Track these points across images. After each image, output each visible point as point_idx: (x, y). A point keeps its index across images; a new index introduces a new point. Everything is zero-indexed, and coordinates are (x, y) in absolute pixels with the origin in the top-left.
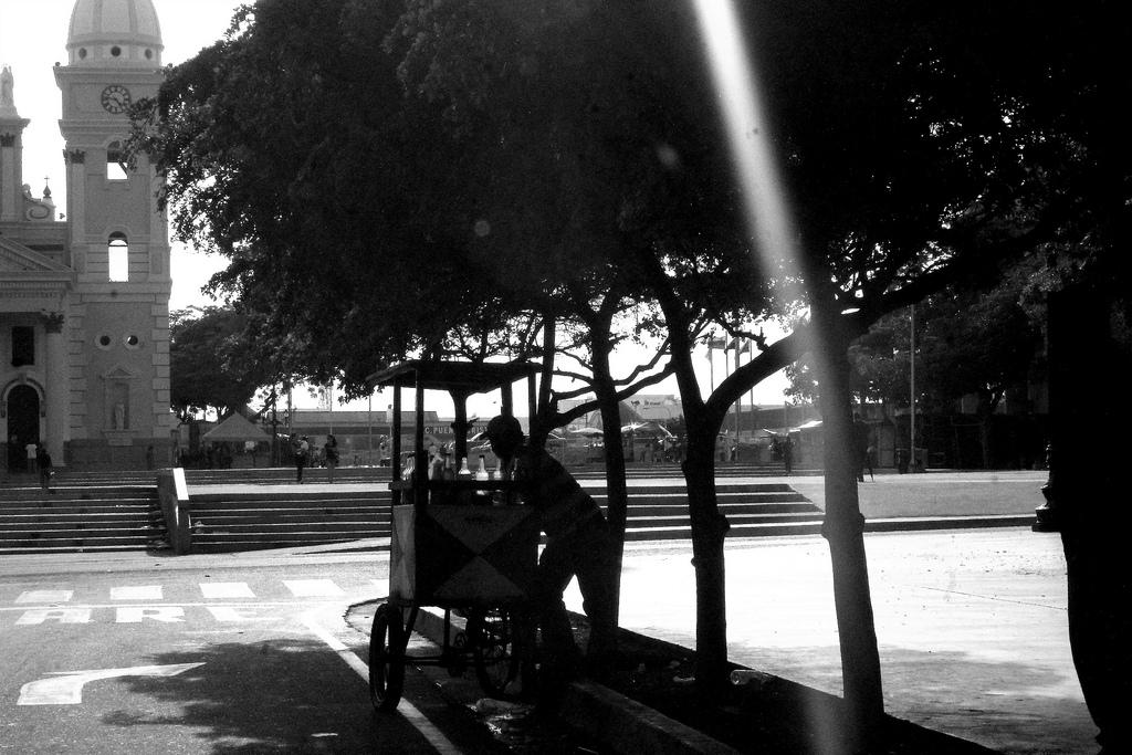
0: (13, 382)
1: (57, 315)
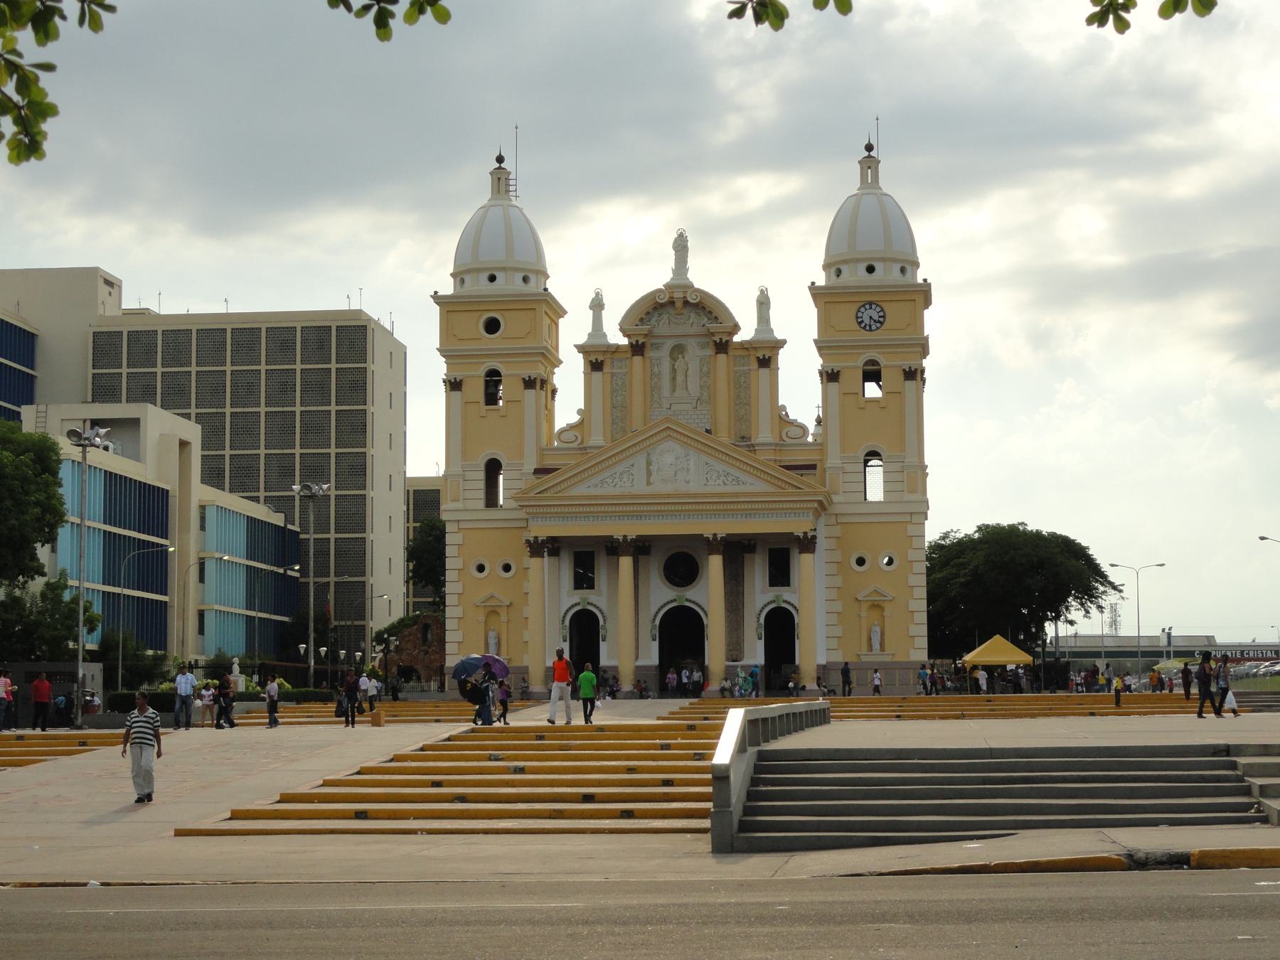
0: (769, 604)
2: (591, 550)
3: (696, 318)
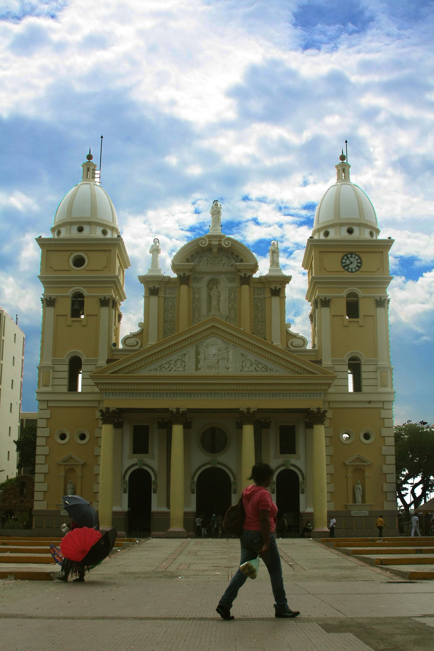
1: (322, 410)
2: (148, 424)
3: (227, 261)
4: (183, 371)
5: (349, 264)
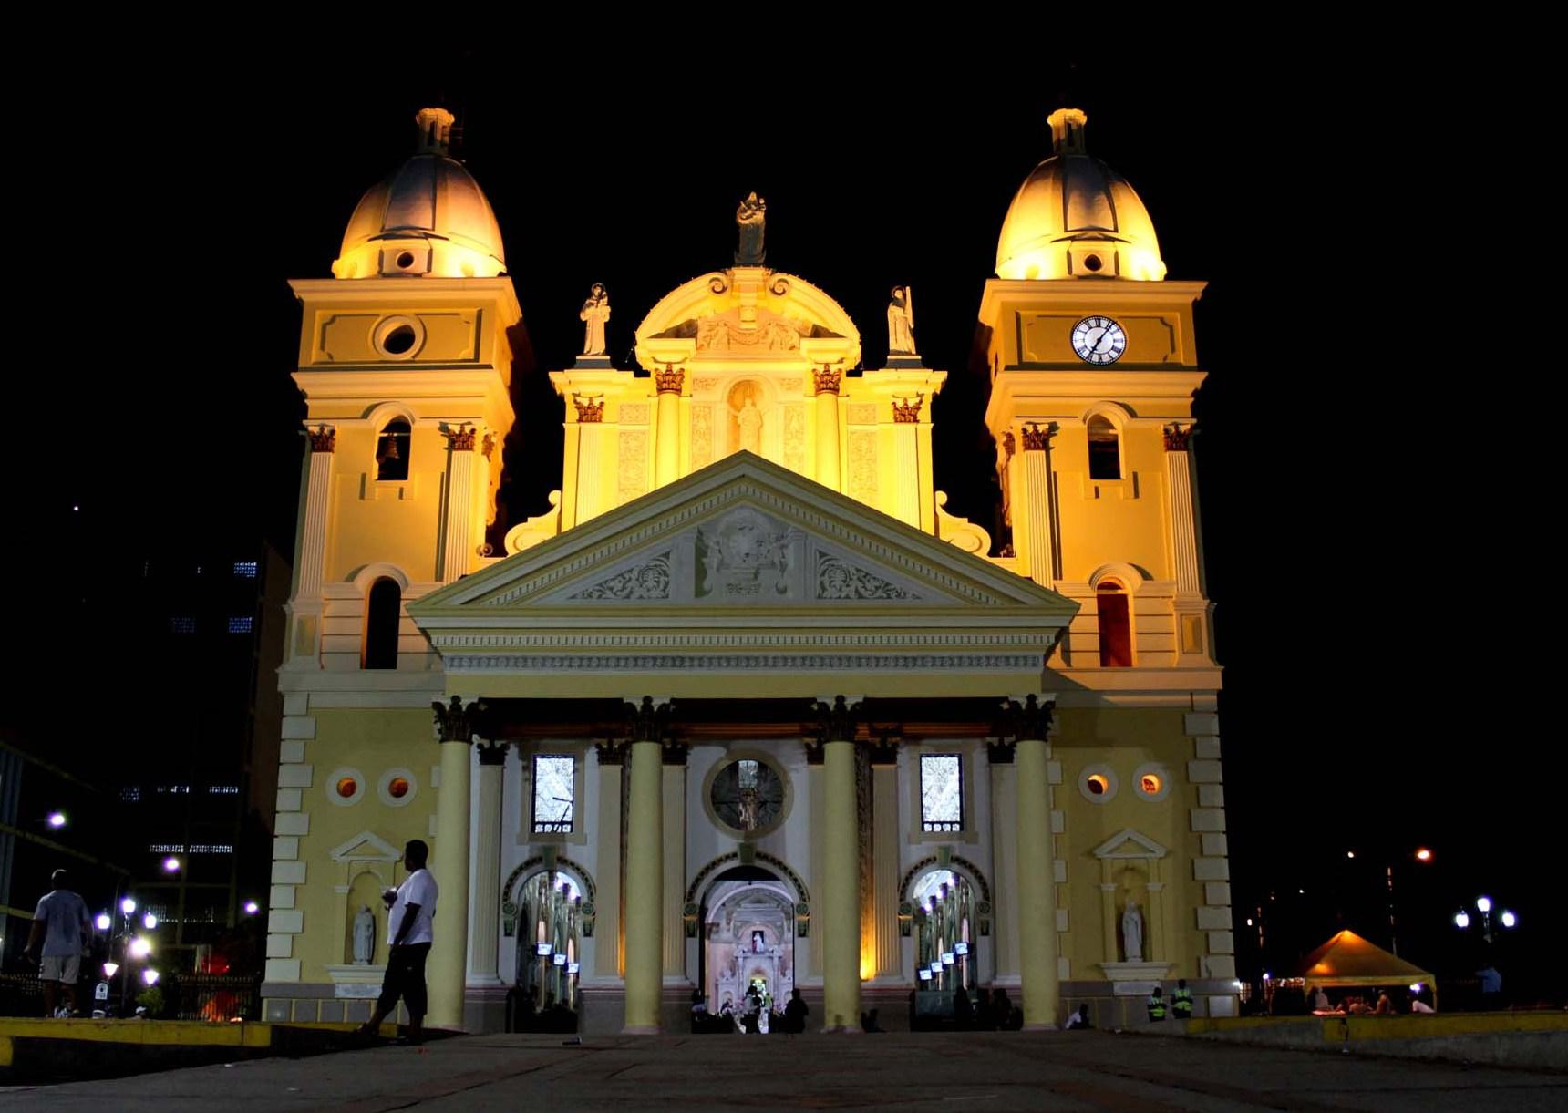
1: (1041, 700)
4: (663, 597)
5: (1096, 346)
